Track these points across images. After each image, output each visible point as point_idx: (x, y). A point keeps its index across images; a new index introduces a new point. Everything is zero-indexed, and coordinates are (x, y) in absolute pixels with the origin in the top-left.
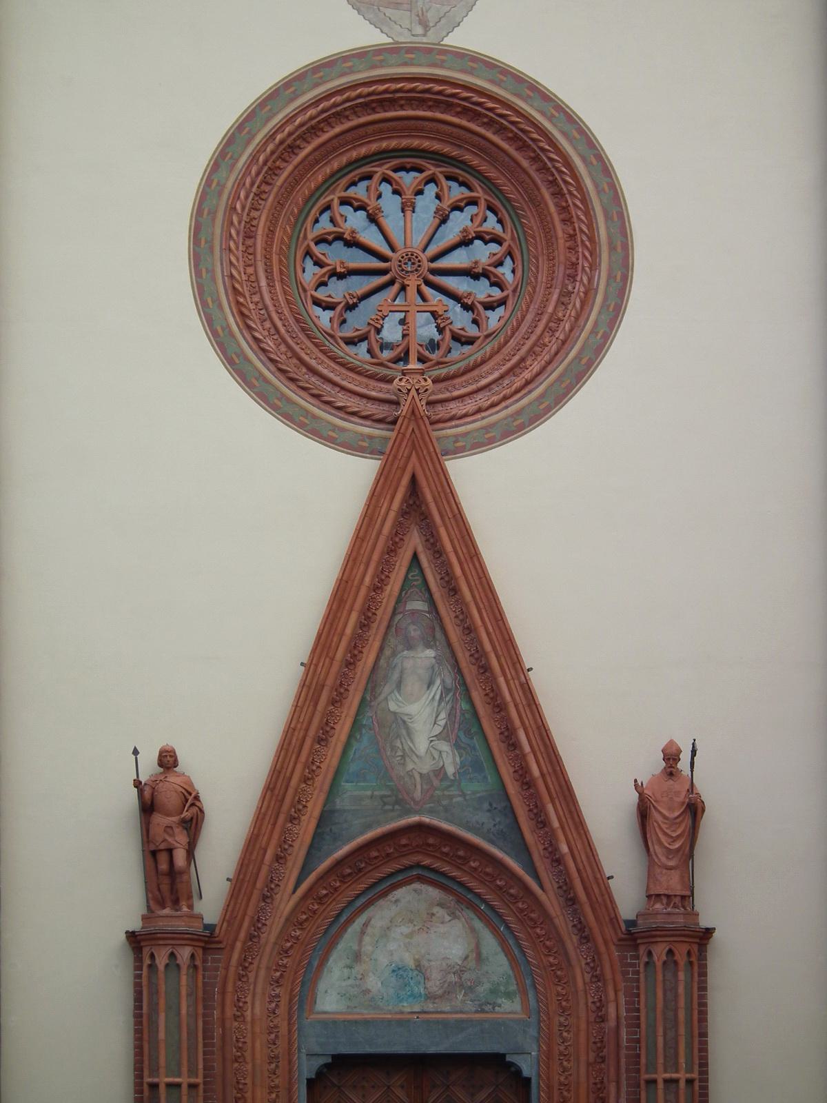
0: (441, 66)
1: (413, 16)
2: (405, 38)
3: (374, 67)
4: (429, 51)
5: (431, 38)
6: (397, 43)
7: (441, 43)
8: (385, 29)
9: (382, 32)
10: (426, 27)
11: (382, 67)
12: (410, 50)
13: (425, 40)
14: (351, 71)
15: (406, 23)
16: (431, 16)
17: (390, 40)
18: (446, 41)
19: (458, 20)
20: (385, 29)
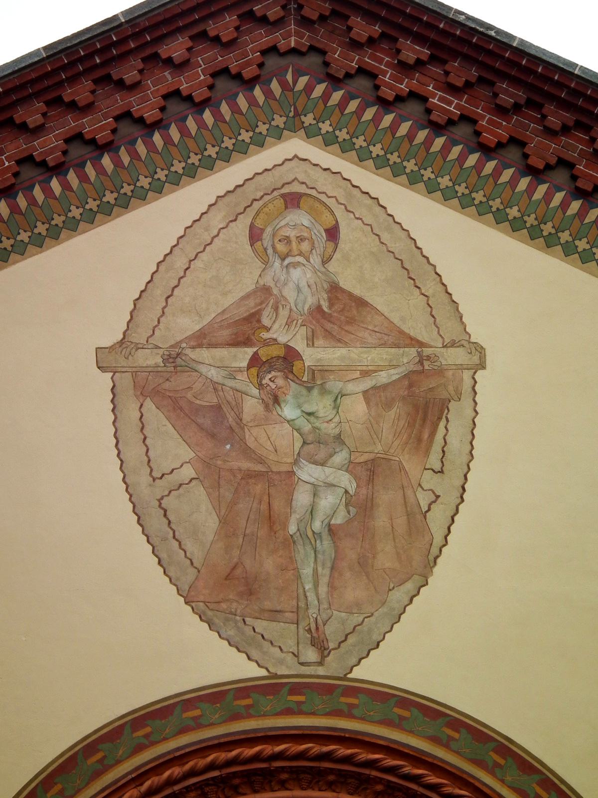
0: (351, 716)
1: (301, 631)
2: (287, 668)
3: (236, 717)
4: (328, 689)
5: (332, 667)
6: (275, 676)
7: (349, 676)
8: (254, 654)
9: (249, 658)
10: (323, 649)
11: (250, 716)
12: (296, 689)
13: (321, 671)
14: (198, 724)
15: (290, 644)
16: (332, 631)
17: (263, 673)
18: (358, 673)
19: (376, 637)
20: (254, 654)
